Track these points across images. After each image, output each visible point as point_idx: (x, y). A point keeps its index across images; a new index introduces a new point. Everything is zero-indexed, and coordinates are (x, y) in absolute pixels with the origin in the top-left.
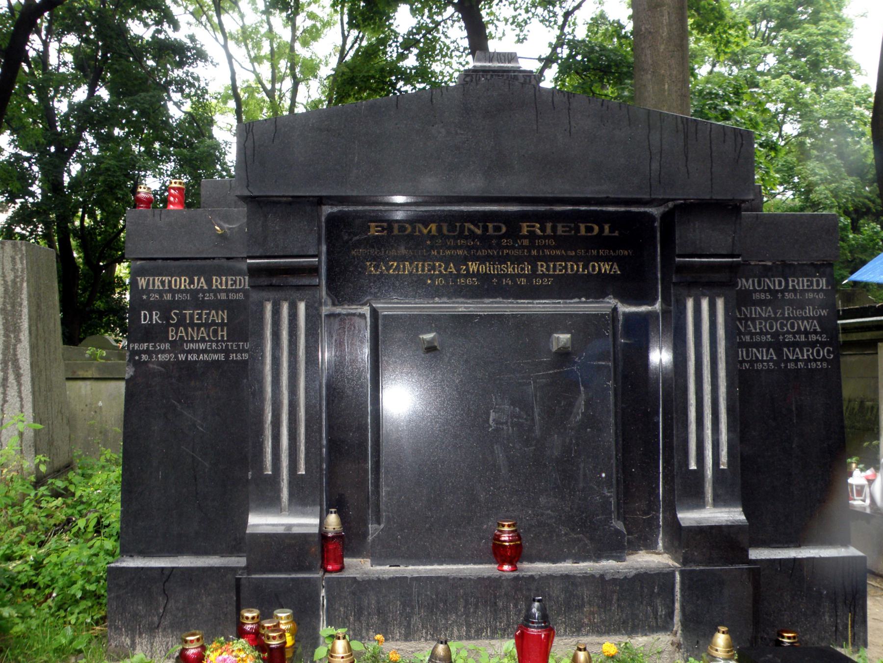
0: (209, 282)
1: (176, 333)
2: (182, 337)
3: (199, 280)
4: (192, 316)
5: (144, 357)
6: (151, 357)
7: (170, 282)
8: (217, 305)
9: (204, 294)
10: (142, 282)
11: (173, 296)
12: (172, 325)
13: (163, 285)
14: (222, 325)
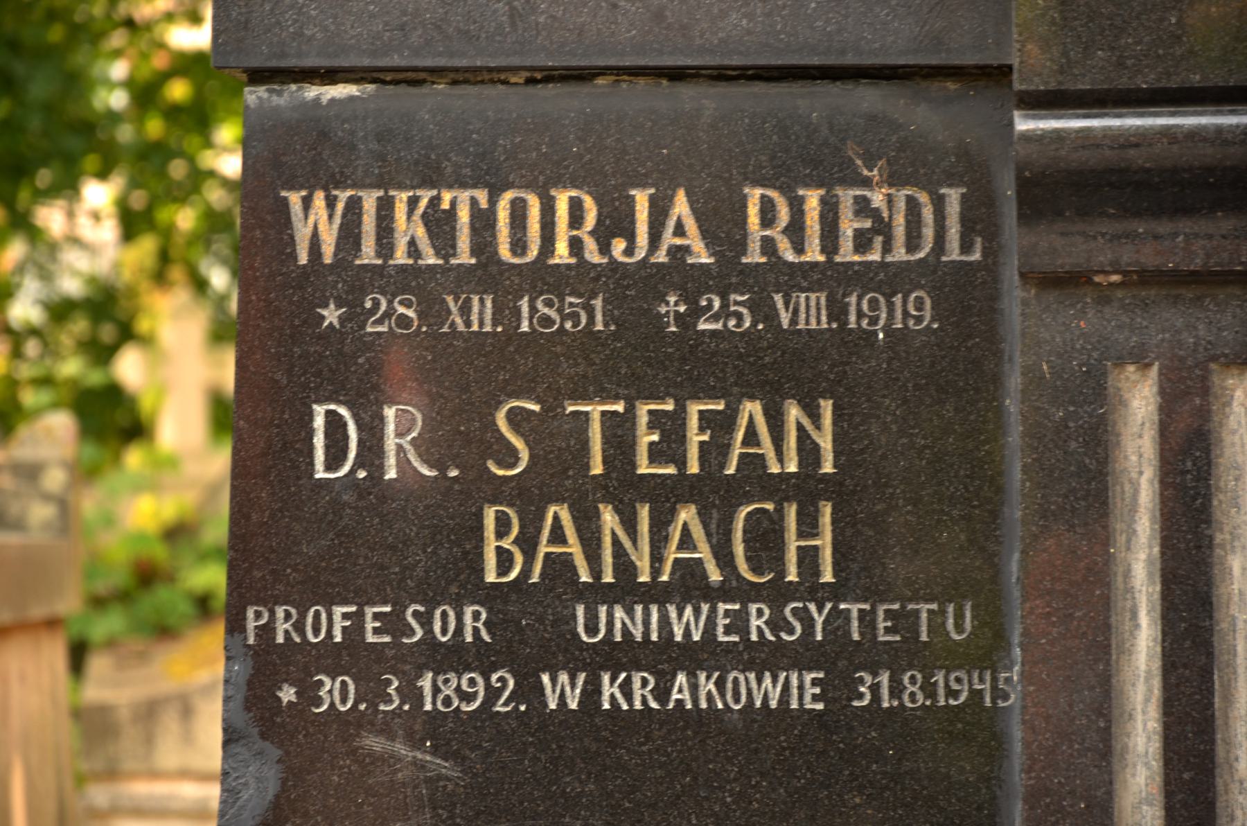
0: (722, 224)
1: (528, 543)
2: (560, 567)
3: (659, 212)
4: (619, 434)
5: (335, 692)
6: (373, 692)
7: (483, 222)
8: (778, 369)
9: (690, 298)
10: (315, 222)
11: (505, 312)
12: (498, 491)
13: (445, 245)
14: (806, 488)
